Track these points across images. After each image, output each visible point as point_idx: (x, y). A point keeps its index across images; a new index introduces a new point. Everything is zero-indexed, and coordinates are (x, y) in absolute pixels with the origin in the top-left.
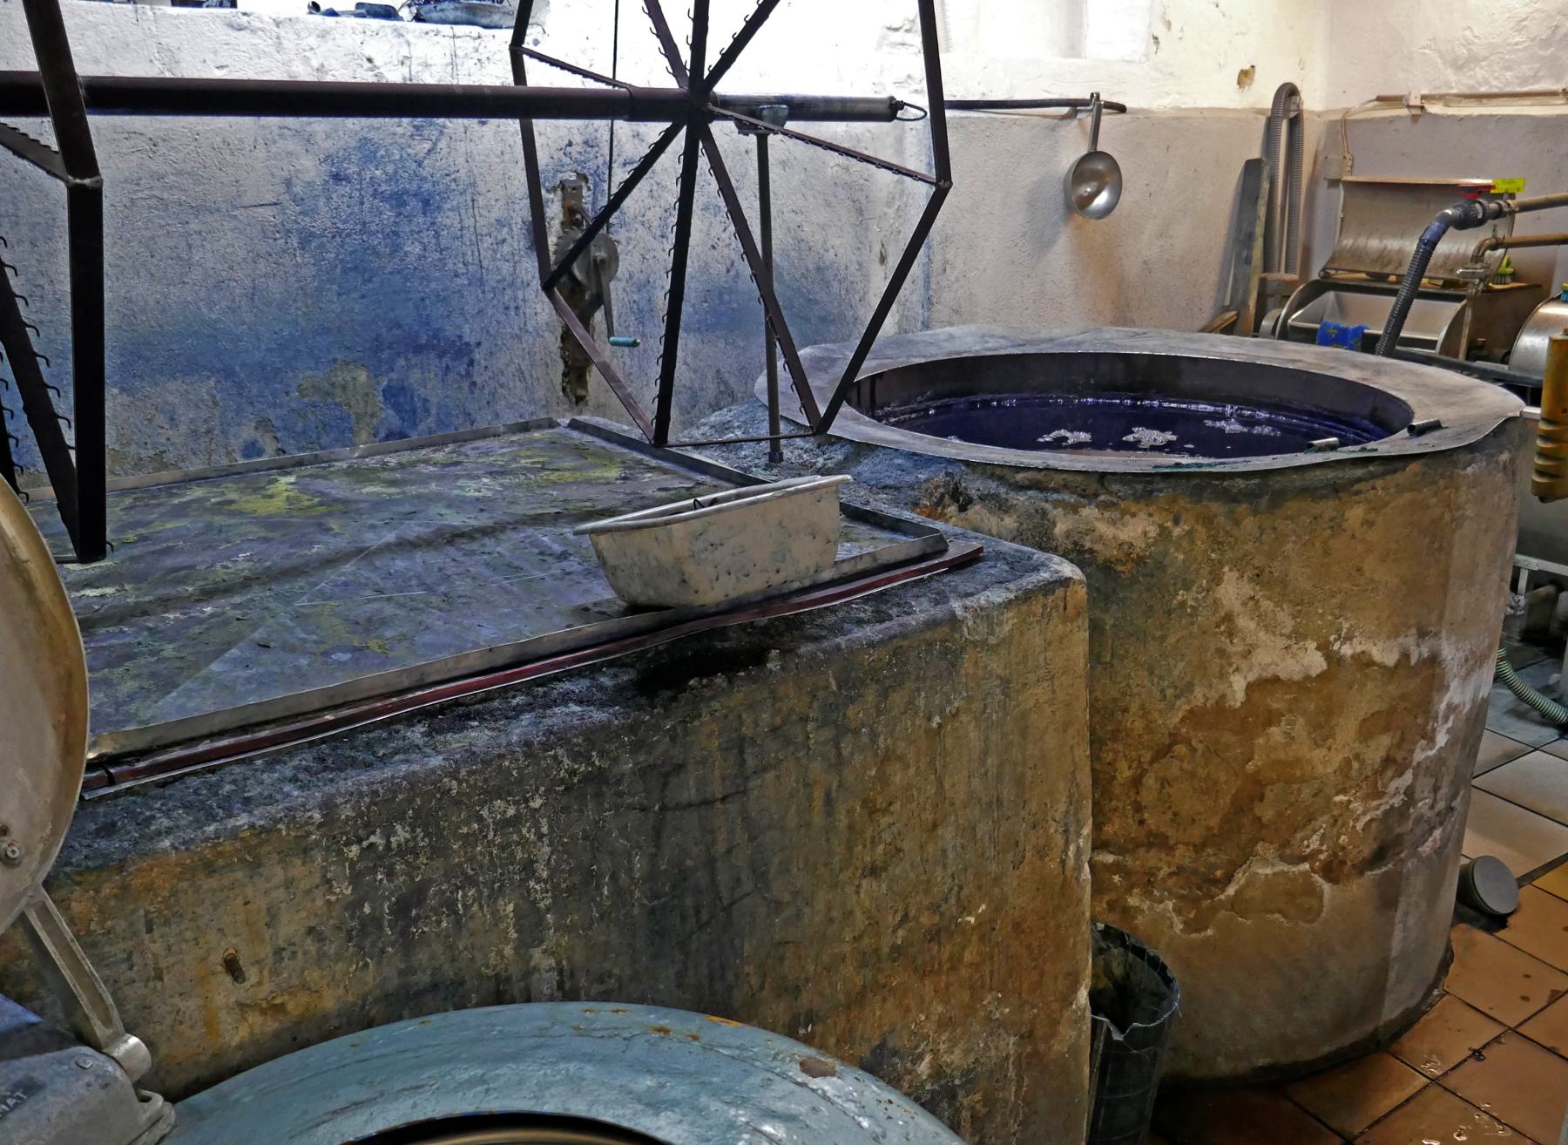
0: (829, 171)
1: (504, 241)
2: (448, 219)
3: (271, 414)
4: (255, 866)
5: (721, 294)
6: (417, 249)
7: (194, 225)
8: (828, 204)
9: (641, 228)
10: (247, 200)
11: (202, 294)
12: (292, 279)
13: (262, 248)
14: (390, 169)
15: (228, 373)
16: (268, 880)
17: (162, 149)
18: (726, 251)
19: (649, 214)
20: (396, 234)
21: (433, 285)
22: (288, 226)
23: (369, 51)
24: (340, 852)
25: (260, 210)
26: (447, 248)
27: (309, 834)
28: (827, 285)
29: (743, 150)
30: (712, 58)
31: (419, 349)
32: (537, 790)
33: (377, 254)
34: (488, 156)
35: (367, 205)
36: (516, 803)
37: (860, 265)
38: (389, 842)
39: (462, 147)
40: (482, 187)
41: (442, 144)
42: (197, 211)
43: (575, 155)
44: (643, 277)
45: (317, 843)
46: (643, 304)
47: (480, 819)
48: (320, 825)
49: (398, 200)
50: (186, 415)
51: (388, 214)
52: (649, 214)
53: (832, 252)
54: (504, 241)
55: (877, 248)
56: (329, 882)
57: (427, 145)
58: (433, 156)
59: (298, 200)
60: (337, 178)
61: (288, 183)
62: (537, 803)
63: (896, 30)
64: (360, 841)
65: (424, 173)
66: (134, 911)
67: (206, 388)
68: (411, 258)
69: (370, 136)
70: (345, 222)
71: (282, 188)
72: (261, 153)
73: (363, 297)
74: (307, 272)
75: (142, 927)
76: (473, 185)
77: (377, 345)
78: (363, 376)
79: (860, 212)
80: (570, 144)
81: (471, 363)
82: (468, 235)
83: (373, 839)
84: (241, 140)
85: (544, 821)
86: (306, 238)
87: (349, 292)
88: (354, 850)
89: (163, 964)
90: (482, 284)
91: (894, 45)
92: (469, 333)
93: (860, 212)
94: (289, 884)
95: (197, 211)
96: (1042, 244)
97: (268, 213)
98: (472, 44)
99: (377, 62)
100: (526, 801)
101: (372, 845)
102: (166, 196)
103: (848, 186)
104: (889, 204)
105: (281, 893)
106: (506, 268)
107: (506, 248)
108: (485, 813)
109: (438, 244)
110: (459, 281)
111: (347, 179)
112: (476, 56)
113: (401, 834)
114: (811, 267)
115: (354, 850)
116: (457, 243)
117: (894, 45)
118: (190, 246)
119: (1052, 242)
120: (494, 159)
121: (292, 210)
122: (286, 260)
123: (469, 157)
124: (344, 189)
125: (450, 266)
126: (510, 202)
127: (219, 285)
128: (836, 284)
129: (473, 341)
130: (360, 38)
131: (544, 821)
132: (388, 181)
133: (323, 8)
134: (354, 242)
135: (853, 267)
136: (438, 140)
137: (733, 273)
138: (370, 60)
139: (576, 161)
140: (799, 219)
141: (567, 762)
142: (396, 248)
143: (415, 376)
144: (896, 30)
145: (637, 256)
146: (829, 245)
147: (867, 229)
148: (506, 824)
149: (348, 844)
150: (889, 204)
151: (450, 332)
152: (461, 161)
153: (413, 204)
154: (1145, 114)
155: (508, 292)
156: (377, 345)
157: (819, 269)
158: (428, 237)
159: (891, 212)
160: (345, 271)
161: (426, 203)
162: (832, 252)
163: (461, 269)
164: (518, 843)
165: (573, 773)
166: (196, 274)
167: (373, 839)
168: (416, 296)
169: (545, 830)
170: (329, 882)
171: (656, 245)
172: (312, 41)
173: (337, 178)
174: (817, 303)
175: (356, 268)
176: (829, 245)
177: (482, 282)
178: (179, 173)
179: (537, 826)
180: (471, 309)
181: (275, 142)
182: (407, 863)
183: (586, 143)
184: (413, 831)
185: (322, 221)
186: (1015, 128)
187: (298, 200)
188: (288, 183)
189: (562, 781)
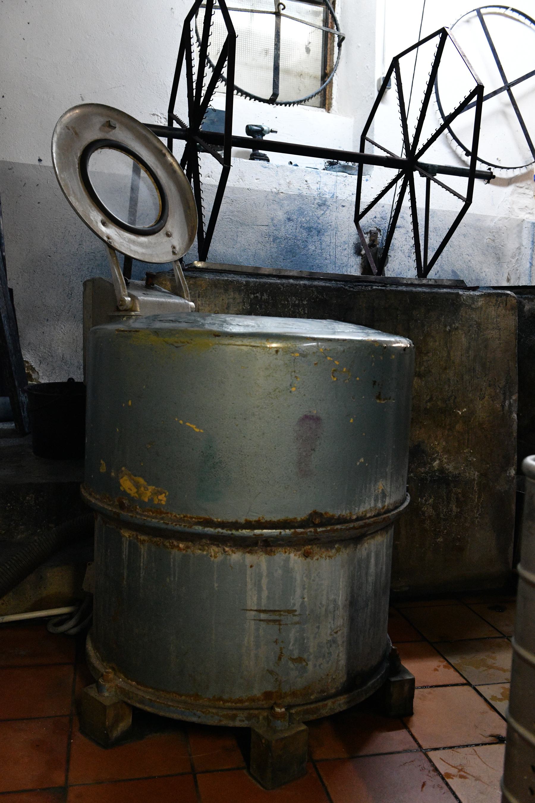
0: (485, 241)
1: (346, 249)
2: (326, 239)
4: (226, 290)
6: (313, 248)
7: (240, 229)
9: (400, 252)
11: (239, 252)
12: (269, 252)
13: (260, 240)
14: (308, 219)
16: (229, 295)
17: (234, 203)
19: (404, 247)
20: (306, 241)
21: (317, 261)
22: (270, 234)
23: (306, 179)
24: (248, 295)
25: (262, 227)
26: (324, 249)
27: (241, 287)
32: (305, 298)
33: (299, 247)
34: (344, 218)
35: (298, 230)
36: (299, 300)
38: (261, 298)
39: (334, 214)
41: (327, 212)
42: (242, 224)
43: (377, 221)
44: (399, 271)
45: (243, 290)
47: (288, 301)
48: (245, 285)
49: (309, 229)
51: (305, 234)
52: (404, 247)
53: (484, 274)
54: (346, 249)
55: (506, 275)
56: (244, 302)
57: (322, 212)
58: (324, 216)
59: (275, 226)
60: (289, 219)
61: (272, 219)
62: (305, 303)
64: (254, 294)
65: (320, 222)
66: (196, 290)
68: (311, 251)
69: (302, 207)
70: (290, 234)
71: (270, 221)
72: (265, 208)
73: (292, 262)
75: (197, 295)
76: (337, 228)
79: (499, 259)
80: (375, 217)
83: (257, 295)
84: (260, 203)
85: (306, 309)
86: (275, 239)
87: (286, 259)
88: (252, 296)
89: (200, 308)
90: (335, 264)
91: (520, 193)
93: (499, 259)
94: (234, 299)
95: (242, 224)
97: (265, 228)
98: (342, 179)
99: (309, 182)
100: (302, 301)
101: (257, 297)
102: (233, 218)
103: (495, 248)
104: (513, 257)
105: (231, 301)
107: (346, 252)
108: (289, 299)
109: (321, 247)
110: (327, 261)
111: (292, 220)
112: (344, 183)
113: (265, 297)
114: (474, 278)
115: (252, 296)
116: (328, 248)
117: (520, 193)
118: (237, 236)
120: (345, 220)
122: (268, 245)
125: (324, 255)
126: (350, 235)
127: (244, 250)
130: (304, 173)
131: (306, 309)
132: (306, 223)
133: (293, 164)
134: (291, 243)
136: (326, 211)
137: (437, 275)
138: (306, 181)
139: (377, 224)
140: (469, 258)
141: (316, 293)
142: (306, 246)
145: (397, 262)
146: (483, 271)
147: (502, 267)
148: (294, 305)
149: (251, 293)
150: (513, 257)
152: (334, 219)
155: (345, 268)
157: (477, 280)
158: (317, 244)
159: (514, 261)
160: (287, 252)
161: (319, 232)
162: (484, 274)
163: (328, 257)
164: (298, 313)
165: (317, 297)
166: (238, 245)
167: (257, 295)
168: (311, 264)
169: (306, 312)
170: (244, 302)
171: (406, 259)
172: (288, 173)
173: (289, 219)
175: (291, 251)
176: (483, 271)
177: (335, 263)
178: (238, 212)
179: (304, 309)
181: (270, 205)
182: (265, 305)
183: (382, 217)
184: (269, 297)
185: (282, 233)
188: (272, 219)
189: (313, 299)
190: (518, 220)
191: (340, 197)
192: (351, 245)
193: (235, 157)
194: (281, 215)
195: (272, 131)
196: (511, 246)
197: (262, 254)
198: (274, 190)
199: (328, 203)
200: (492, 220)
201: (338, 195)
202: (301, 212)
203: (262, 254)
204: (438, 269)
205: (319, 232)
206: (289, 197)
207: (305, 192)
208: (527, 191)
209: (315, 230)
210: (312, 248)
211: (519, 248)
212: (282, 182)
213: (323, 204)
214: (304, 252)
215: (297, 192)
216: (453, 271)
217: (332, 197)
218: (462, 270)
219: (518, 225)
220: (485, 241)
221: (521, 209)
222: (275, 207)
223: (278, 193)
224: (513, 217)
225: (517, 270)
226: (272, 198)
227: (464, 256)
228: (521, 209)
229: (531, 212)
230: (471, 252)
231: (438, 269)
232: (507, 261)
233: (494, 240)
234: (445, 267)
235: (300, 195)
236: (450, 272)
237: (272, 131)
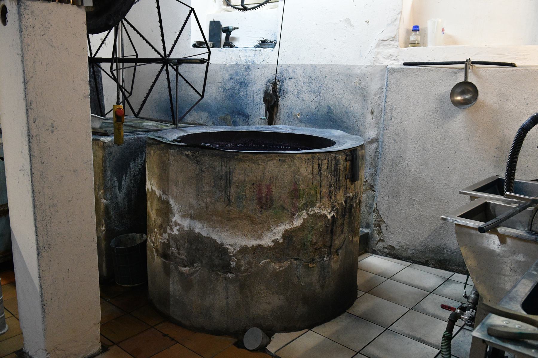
0: (353, 84)
2: (249, 88)
3: (215, 121)
5: (312, 115)
8: (352, 93)
10: (217, 82)
13: (218, 90)
15: (210, 112)
18: (316, 103)
23: (240, 54)
28: (349, 117)
29: (324, 76)
30: (167, 53)
31: (240, 114)
37: (363, 113)
39: (254, 73)
40: (256, 82)
46: (290, 113)
49: (241, 83)
50: (204, 118)
53: (352, 108)
55: (370, 109)
59: (224, 82)
60: (231, 78)
63: (386, 40)
67: (206, 114)
74: (224, 96)
77: (233, 112)
78: (230, 118)
79: (364, 97)
81: (249, 119)
82: (252, 92)
86: (225, 89)
91: (385, 45)
92: (249, 112)
93: (364, 97)
96: (447, 117)
103: (361, 89)
104: (375, 95)
106: (259, 100)
107: (259, 96)
117: (385, 45)
119: (452, 117)
121: (223, 84)
123: (255, 75)
124: (232, 81)
128: (353, 118)
129: (250, 114)
135: (360, 114)
140: (340, 97)
143: (238, 119)
144: (386, 40)
146: (351, 106)
147: (367, 102)
150: (375, 95)
151: (245, 112)
153: (243, 85)
154: (525, 68)
156: (233, 112)
157: (346, 112)
158: (245, 91)
159: (376, 98)
161: (246, 84)
162: (352, 108)
171: (295, 99)
172: (231, 53)
174: (345, 122)
176: (351, 106)
180: (250, 108)
186: (432, 72)
187: (224, 82)
190: (382, 66)
191: (257, 63)
192: (262, 91)
193: (213, 47)
194: (227, 76)
195: (235, 29)
196: (374, 86)
197: (219, 98)
198: (224, 63)
199: (250, 67)
200: (359, 68)
201: (256, 62)
202: (237, 74)
203: (219, 98)
204: (318, 105)
205: (246, 84)
206: (231, 66)
207: (239, 62)
208: (392, 43)
209: (244, 84)
210: (242, 94)
211: (381, 88)
212: (228, 58)
213: (248, 68)
214: (238, 96)
215: (234, 63)
216: (328, 106)
217: (253, 63)
218: (335, 106)
219: (382, 70)
220: (353, 84)
221: (386, 57)
222: (225, 72)
223: (226, 65)
224: (377, 64)
225: (380, 105)
226: (223, 67)
227: (337, 95)
228: (386, 57)
229: (396, 58)
230: (342, 92)
231: (318, 105)
232: (371, 98)
233: (360, 83)
234: (323, 104)
235: (237, 65)
236: (326, 106)
237: (235, 29)
